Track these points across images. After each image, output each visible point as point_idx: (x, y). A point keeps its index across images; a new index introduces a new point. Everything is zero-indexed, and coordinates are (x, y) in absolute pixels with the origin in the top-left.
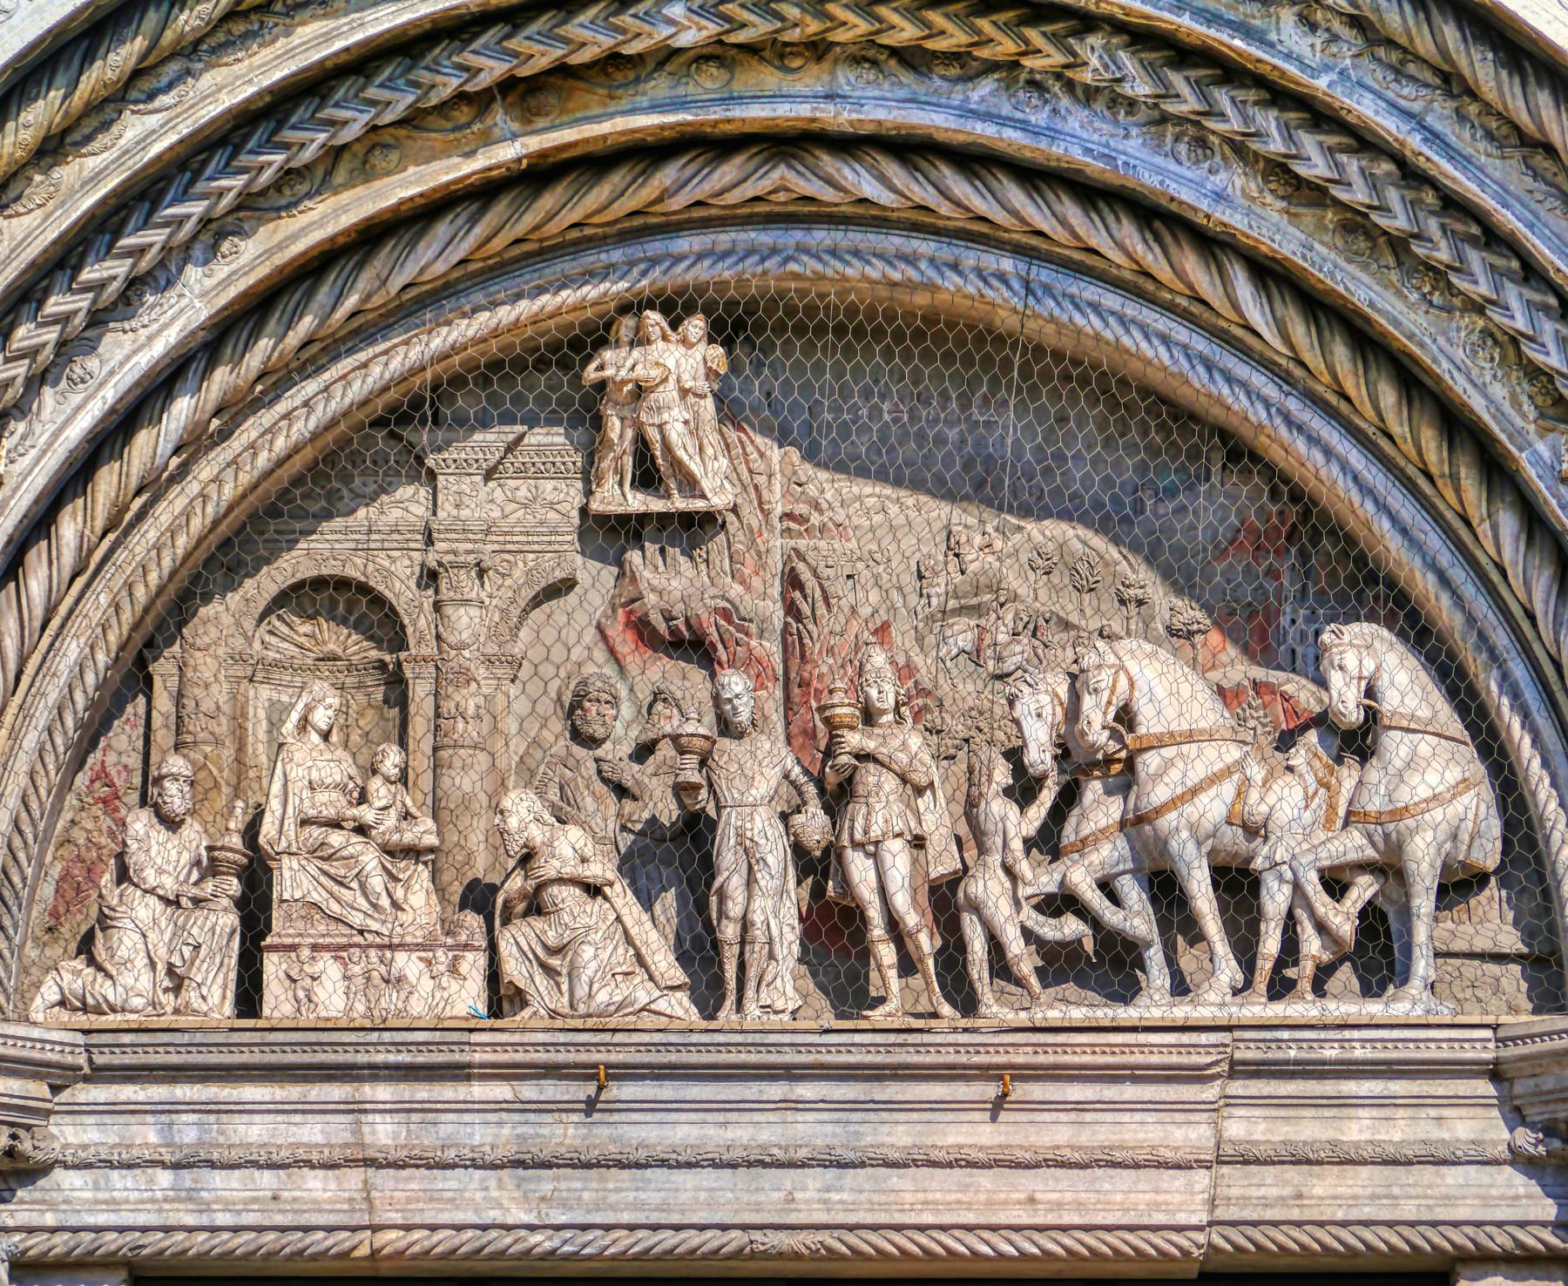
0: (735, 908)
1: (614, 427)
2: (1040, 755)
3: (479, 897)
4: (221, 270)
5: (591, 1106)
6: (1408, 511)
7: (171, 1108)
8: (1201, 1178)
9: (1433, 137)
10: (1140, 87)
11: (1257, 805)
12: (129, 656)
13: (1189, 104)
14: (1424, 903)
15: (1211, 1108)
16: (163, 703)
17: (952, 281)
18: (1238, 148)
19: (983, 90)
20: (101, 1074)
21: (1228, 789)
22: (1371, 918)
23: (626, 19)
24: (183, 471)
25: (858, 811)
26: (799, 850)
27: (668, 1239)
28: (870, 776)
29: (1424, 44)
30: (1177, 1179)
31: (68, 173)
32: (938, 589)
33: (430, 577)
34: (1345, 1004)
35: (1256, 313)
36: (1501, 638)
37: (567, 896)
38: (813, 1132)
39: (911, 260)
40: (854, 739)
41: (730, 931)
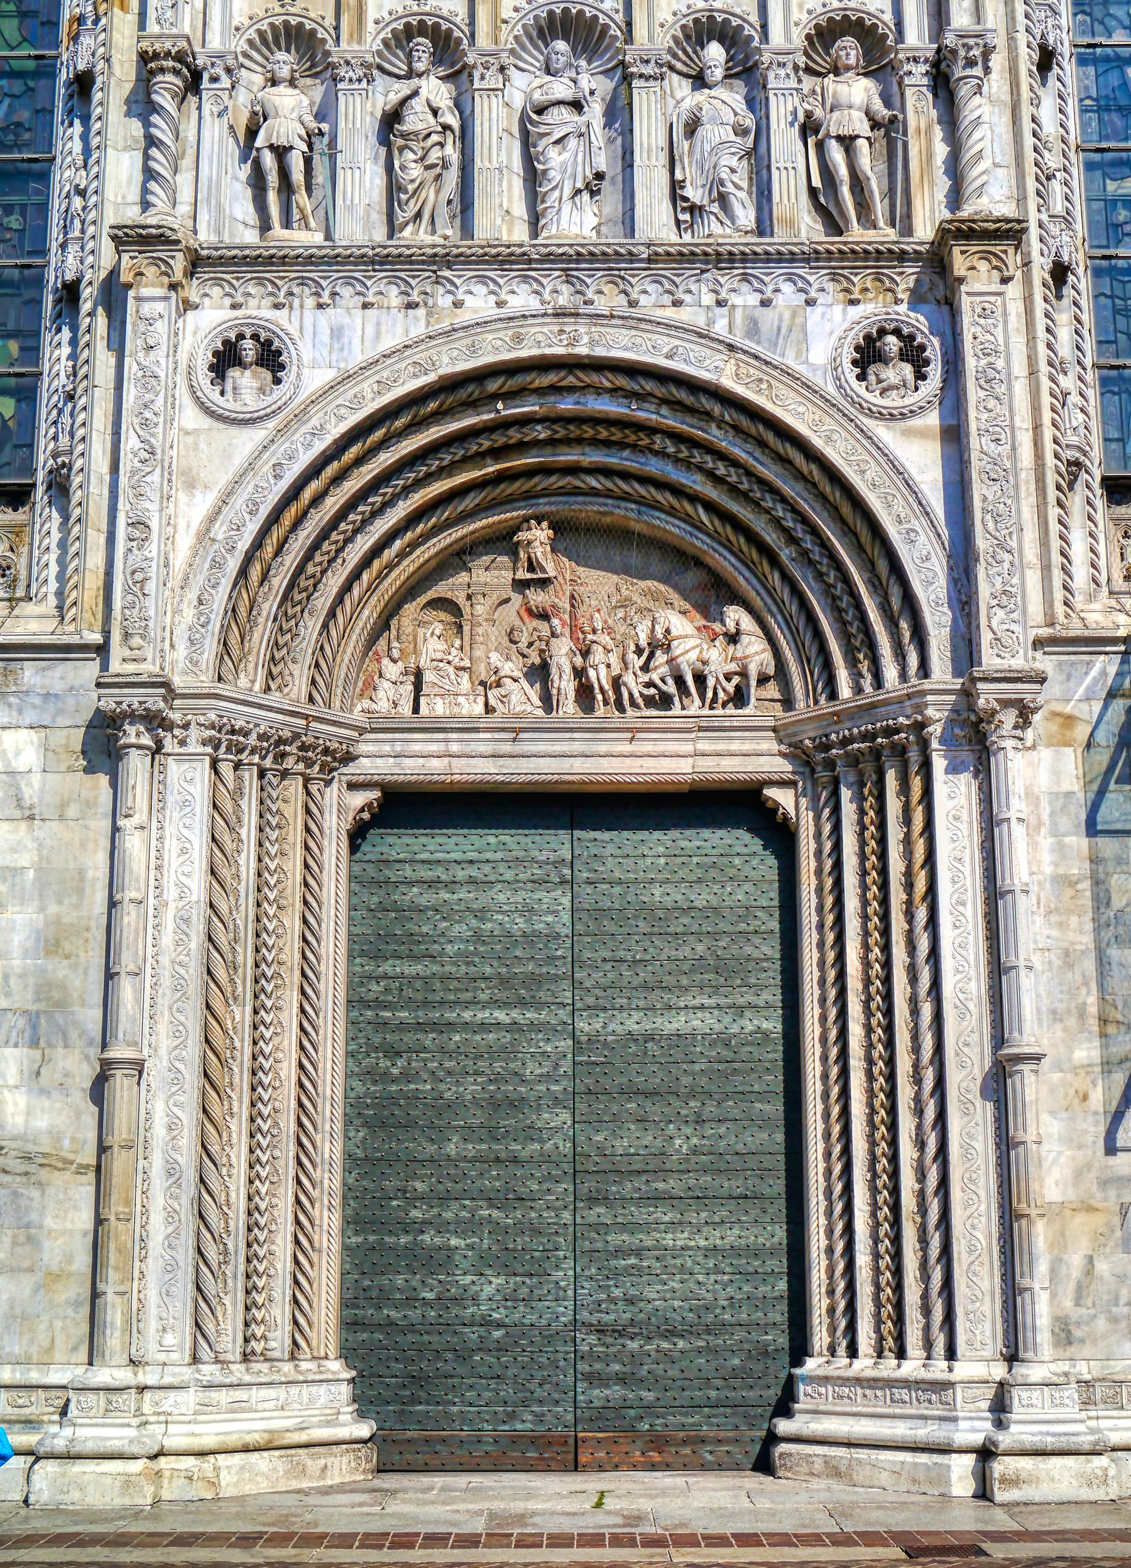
0: (556, 685)
1: (522, 554)
2: (643, 642)
3: (483, 683)
4: (409, 502)
5: (514, 740)
6: (747, 574)
7: (394, 741)
8: (690, 760)
9: (755, 459)
10: (671, 450)
11: (705, 656)
12: (384, 616)
13: (685, 453)
14: (753, 683)
15: (693, 740)
16: (394, 632)
17: (617, 511)
18: (700, 469)
19: (626, 453)
20: (373, 730)
21: (697, 651)
22: (738, 688)
23: (525, 430)
24: (398, 563)
25: (591, 657)
26: (574, 668)
27: (537, 777)
28: (595, 647)
29: (753, 431)
30: (682, 761)
31: (364, 469)
32: (614, 601)
33: (469, 597)
34: (731, 710)
35: (704, 518)
36: (774, 609)
37: (508, 681)
38: (578, 747)
39: (606, 505)
40: (590, 637)
41: (554, 692)
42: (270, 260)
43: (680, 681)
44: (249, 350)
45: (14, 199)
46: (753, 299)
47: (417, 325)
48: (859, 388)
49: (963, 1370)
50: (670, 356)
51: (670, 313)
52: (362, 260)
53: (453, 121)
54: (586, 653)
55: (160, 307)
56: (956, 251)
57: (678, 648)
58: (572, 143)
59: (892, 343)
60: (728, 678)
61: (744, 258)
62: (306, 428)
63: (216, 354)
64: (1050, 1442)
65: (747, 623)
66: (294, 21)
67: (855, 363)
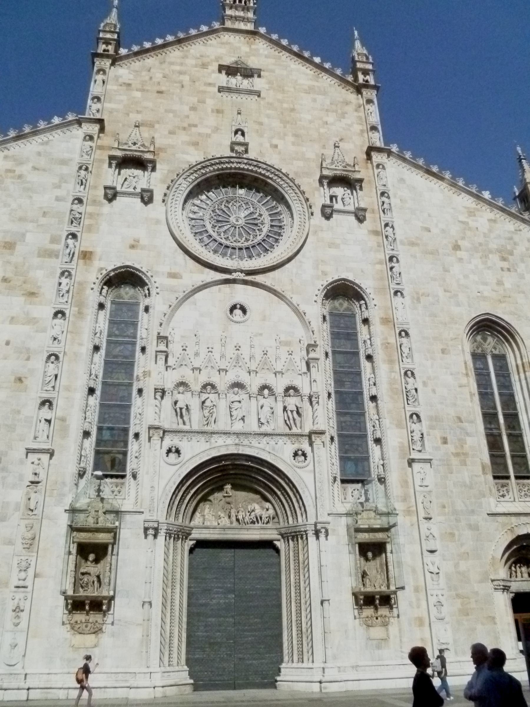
38: (237, 532)
42: (179, 432)
43: (257, 518)
44: (174, 449)
45: (123, 412)
46: (274, 443)
47: (207, 446)
48: (294, 461)
49: (315, 665)
50: (257, 454)
51: (257, 445)
52: (198, 432)
53: (215, 404)
54: (238, 512)
55: (157, 441)
56: (313, 436)
57: (257, 511)
58: (239, 409)
59: (300, 453)
60: (266, 518)
61: (272, 435)
62: (185, 467)
63: (167, 450)
64: (332, 680)
65: (270, 506)
66: (184, 381)
67: (293, 456)
